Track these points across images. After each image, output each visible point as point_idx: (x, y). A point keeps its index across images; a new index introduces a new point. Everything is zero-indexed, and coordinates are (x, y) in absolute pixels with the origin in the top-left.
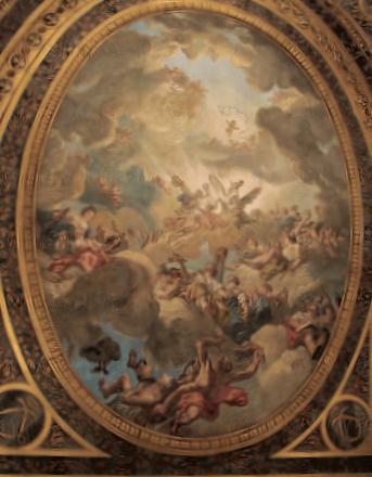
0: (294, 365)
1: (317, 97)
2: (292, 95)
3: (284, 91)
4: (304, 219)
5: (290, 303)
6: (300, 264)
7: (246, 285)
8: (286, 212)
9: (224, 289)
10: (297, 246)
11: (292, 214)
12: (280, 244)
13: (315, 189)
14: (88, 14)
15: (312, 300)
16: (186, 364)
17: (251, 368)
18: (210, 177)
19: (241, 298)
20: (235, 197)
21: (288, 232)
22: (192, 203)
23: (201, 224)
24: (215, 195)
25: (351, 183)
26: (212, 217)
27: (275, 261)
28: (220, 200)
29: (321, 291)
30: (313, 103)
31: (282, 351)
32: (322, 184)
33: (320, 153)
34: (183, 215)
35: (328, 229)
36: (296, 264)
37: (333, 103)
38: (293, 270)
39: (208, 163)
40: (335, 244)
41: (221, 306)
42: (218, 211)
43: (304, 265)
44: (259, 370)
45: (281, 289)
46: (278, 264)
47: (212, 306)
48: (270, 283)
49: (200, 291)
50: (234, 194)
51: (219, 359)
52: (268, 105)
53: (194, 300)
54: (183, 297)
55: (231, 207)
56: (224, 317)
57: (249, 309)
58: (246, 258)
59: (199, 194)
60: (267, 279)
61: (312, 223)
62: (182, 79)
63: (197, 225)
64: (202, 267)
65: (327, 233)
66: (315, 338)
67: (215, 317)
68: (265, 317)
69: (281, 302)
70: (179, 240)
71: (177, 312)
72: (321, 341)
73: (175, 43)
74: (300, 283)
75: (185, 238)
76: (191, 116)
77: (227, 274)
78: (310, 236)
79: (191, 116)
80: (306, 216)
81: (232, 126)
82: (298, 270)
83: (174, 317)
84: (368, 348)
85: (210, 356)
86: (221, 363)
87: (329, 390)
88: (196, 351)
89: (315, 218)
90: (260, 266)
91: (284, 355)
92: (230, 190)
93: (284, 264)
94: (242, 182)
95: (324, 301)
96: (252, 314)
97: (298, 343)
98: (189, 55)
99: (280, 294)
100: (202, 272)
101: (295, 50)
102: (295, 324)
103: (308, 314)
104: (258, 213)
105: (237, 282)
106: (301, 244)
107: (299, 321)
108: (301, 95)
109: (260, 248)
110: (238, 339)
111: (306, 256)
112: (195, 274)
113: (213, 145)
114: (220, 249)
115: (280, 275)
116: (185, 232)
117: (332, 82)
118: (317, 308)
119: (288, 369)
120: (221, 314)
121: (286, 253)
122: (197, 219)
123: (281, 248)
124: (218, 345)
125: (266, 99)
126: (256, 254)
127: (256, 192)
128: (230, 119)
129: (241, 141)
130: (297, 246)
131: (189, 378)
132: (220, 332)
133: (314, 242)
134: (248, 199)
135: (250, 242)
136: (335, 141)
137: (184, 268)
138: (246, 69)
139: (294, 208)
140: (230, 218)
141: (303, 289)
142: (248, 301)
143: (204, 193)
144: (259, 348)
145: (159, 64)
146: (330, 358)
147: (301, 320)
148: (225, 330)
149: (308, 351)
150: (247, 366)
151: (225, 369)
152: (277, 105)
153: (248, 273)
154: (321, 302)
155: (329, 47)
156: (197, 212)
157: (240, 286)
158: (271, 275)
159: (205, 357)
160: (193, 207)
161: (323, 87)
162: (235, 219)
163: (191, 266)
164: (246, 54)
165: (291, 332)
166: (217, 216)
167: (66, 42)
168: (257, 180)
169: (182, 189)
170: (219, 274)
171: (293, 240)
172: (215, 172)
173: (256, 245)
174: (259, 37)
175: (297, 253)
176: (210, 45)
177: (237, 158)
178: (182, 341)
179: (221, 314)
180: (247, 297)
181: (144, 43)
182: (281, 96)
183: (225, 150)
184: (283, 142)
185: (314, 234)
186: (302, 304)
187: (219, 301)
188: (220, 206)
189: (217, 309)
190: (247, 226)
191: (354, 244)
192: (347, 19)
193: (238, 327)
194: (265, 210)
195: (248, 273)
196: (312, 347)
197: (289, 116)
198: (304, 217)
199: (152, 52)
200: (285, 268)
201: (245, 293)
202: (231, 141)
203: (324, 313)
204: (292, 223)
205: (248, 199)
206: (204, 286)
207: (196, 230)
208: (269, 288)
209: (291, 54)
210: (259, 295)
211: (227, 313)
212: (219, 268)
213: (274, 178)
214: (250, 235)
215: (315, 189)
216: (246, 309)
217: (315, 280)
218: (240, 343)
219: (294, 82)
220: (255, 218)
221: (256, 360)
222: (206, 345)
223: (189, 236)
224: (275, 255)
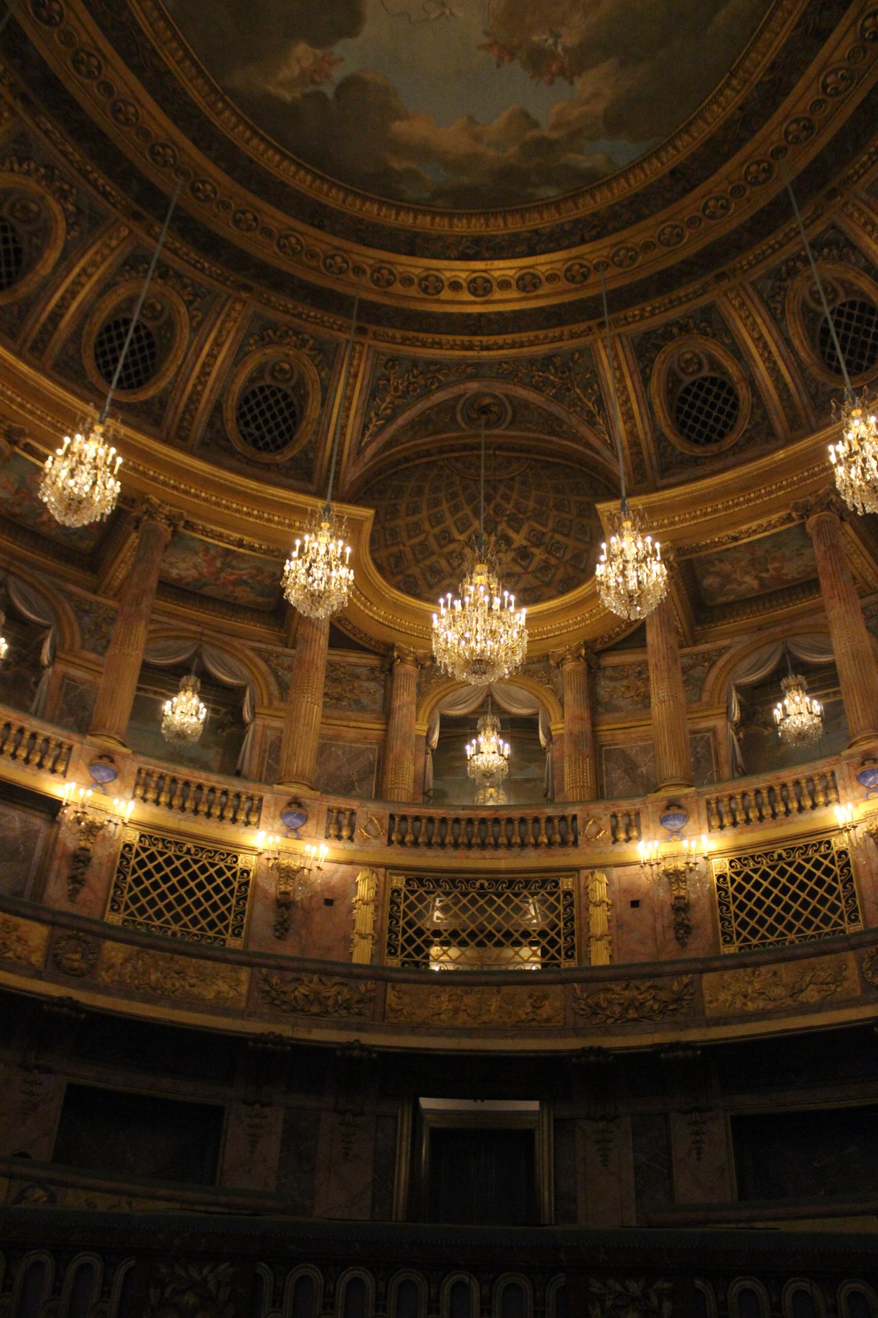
14: (727, 157)
37: (196, 93)
52: (339, 49)
62: (538, 61)
73: (554, 135)
98: (524, 119)
101: (301, 180)
108: (271, 89)
125: (349, 57)
145: (585, 84)
152: (319, 52)
155: (226, 206)
161: (226, 122)
167: (777, 86)
174: (384, 187)
181: (614, 123)
192: (202, 270)
199: (600, 106)
209: (308, 171)
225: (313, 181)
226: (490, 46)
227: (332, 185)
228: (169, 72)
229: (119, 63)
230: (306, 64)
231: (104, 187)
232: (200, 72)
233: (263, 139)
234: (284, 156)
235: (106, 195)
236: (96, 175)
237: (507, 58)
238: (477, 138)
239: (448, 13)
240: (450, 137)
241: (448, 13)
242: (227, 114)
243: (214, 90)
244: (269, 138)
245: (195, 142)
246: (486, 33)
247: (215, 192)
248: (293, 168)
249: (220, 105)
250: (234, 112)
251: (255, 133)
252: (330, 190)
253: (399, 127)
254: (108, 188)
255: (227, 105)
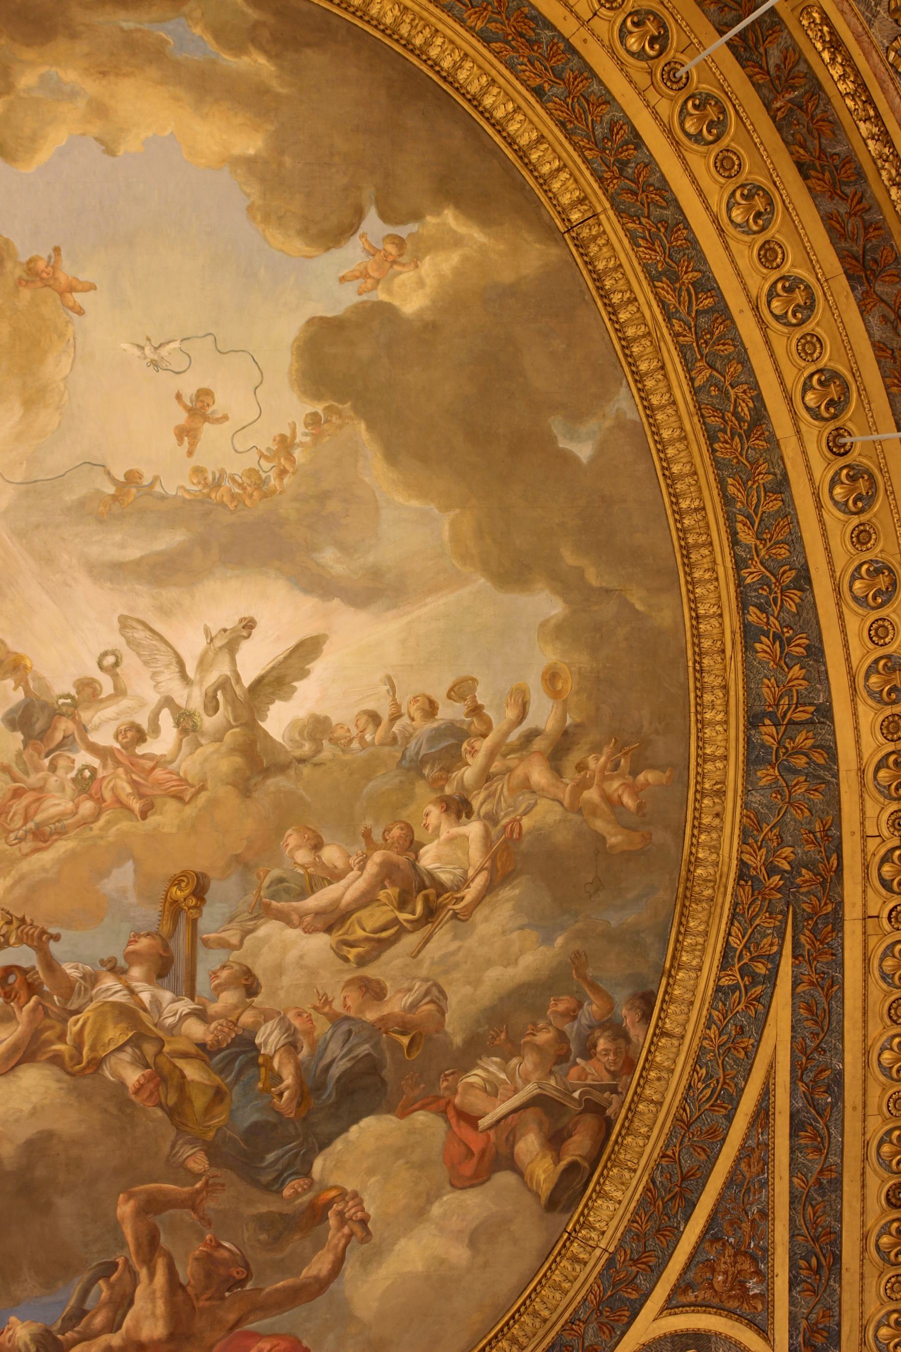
0: (478, 1238)
1: (550, 234)
2: (457, 241)
3: (404, 231)
4: (498, 726)
5: (455, 1028)
6: (489, 889)
7: (283, 992)
8: (431, 708)
9: (201, 1015)
10: (474, 829)
11: (451, 711)
12: (409, 829)
13: (545, 604)
15: (540, 1011)
16: (86, 1276)
17: (320, 1265)
18: (125, 623)
19: (269, 1038)
20: (223, 684)
21: (437, 784)
22: (65, 726)
23: (100, 800)
24: (145, 689)
25: (689, 566)
26: (140, 770)
27: (392, 892)
28: (168, 702)
29: (570, 977)
30: (532, 257)
31: (431, 1197)
32: (566, 584)
33: (567, 458)
34: (33, 779)
35: (596, 749)
36: (470, 894)
37: (615, 244)
38: (462, 918)
39: (114, 572)
40: (627, 800)
41: (192, 1072)
42: (164, 742)
43: (509, 893)
44: (349, 1270)
45: (419, 987)
46: (403, 903)
47: (162, 1077)
48: (371, 972)
49: (115, 1034)
50: (222, 669)
51: (200, 1249)
53: (97, 1064)
54: (56, 1060)
55: (209, 723)
56: (208, 1110)
57: (299, 1068)
58: (277, 899)
59: (88, 690)
60: (362, 961)
61: (531, 736)
63: (87, 807)
64: (116, 951)
65: (595, 764)
66: (555, 1141)
67: (175, 1114)
68: (360, 1089)
69: (420, 1034)
70: (25, 866)
71: (34, 1112)
72: (578, 1146)
74: (496, 951)
75: (47, 857)
76: (33, 400)
77: (209, 962)
78: (526, 785)
79: (33, 400)
80: (511, 714)
81: (200, 408)
82: (479, 915)
83: (25, 1133)
84: (767, 1147)
85: (163, 1239)
86: (208, 1262)
87: (616, 1302)
88: (116, 1227)
89: (544, 715)
90: (333, 920)
91: (436, 1210)
92: (203, 664)
93: (424, 899)
94: (249, 625)
95: (583, 1023)
96: (309, 1087)
97: (488, 1161)
99: (414, 1006)
100: (115, 970)
102: (475, 1101)
103: (529, 1062)
104: (318, 728)
105: (249, 984)
106: (491, 819)
107: (492, 1090)
108: (477, 235)
109: (331, 854)
110: (266, 1178)
111: (507, 860)
112: (92, 979)
113: (129, 499)
114: (176, 881)
115: (411, 940)
116: (42, 836)
117: (618, 157)
118: (562, 1036)
119: (459, 1254)
120: (199, 1102)
121: (429, 858)
122: (86, 784)
123: (412, 846)
124: (192, 1203)
125: (330, 283)
126: (312, 885)
127: (307, 650)
128: (189, 386)
129: (237, 467)
130: (474, 829)
131: (99, 1321)
132: (198, 1162)
133: (544, 804)
134: (275, 683)
135: (292, 839)
136: (624, 403)
137: (50, 964)
138: (249, 163)
139: (461, 690)
140: (209, 761)
141: (498, 978)
142: (292, 1046)
143: (107, 685)
144: (343, 1194)
146: (611, 1210)
147: (498, 1087)
148: (213, 1152)
149: (537, 1195)
150: (305, 1262)
151: (225, 1277)
153: (294, 955)
154: (572, 1015)
156: (83, 758)
157: (257, 1000)
158: (380, 945)
159: (150, 1246)
160: (66, 742)
161: (570, 179)
162: (226, 765)
163: (73, 955)
164: (253, 100)
165: (465, 1132)
166: (158, 762)
168: (310, 603)
169: (22, 682)
170: (180, 968)
171: (459, 808)
172: (142, 601)
173: (317, 846)
175: (476, 854)
176: (92, 87)
177: (243, 530)
178: (65, 1205)
179: (199, 1102)
180: (290, 1031)
182: (403, 252)
183: (174, 512)
184: (408, 443)
185: (539, 775)
186: (500, 1028)
187: (185, 1055)
188: (166, 719)
189: (182, 1083)
190: (276, 782)
191: (701, 793)
193: (261, 1135)
194: (343, 715)
195: (294, 955)
196: (543, 1171)
197: (428, 330)
198: (500, 717)
200: (431, 913)
201: (283, 1019)
202: (198, 471)
203: (588, 1052)
204: (450, 746)
205: (275, 683)
206: (127, 1014)
207: (85, 823)
208: (373, 991)
209: (434, 65)
210: (337, 1020)
211: (219, 1095)
212: (180, 945)
213: (374, 591)
214: (286, 814)
215: (545, 604)
216: (289, 1080)
217: (548, 940)
218: (274, 1187)
219: (449, 189)
220: (307, 747)
221: (334, 1235)
222: (150, 1207)
223: (63, 846)
224: (388, 872)
225: (428, 43)
226: (72, 289)
227: (391, 32)
228: (652, 279)
229: (736, 302)
230: (407, 277)
231: (833, 59)
232: (598, 279)
233: (511, 141)
234: (475, 101)
235: (836, 44)
236: (842, 87)
237: (41, 265)
238: (99, 110)
239: (148, 350)
240: (151, 113)
241: (148, 350)
242: (565, 199)
243: (581, 245)
244: (498, 139)
245: (637, 140)
246: (80, 312)
247: (623, 34)
248: (462, 76)
249: (575, 216)
250: (553, 198)
251: (522, 154)
252: (398, 22)
253: (251, 144)
254: (826, 56)
255: (563, 213)
